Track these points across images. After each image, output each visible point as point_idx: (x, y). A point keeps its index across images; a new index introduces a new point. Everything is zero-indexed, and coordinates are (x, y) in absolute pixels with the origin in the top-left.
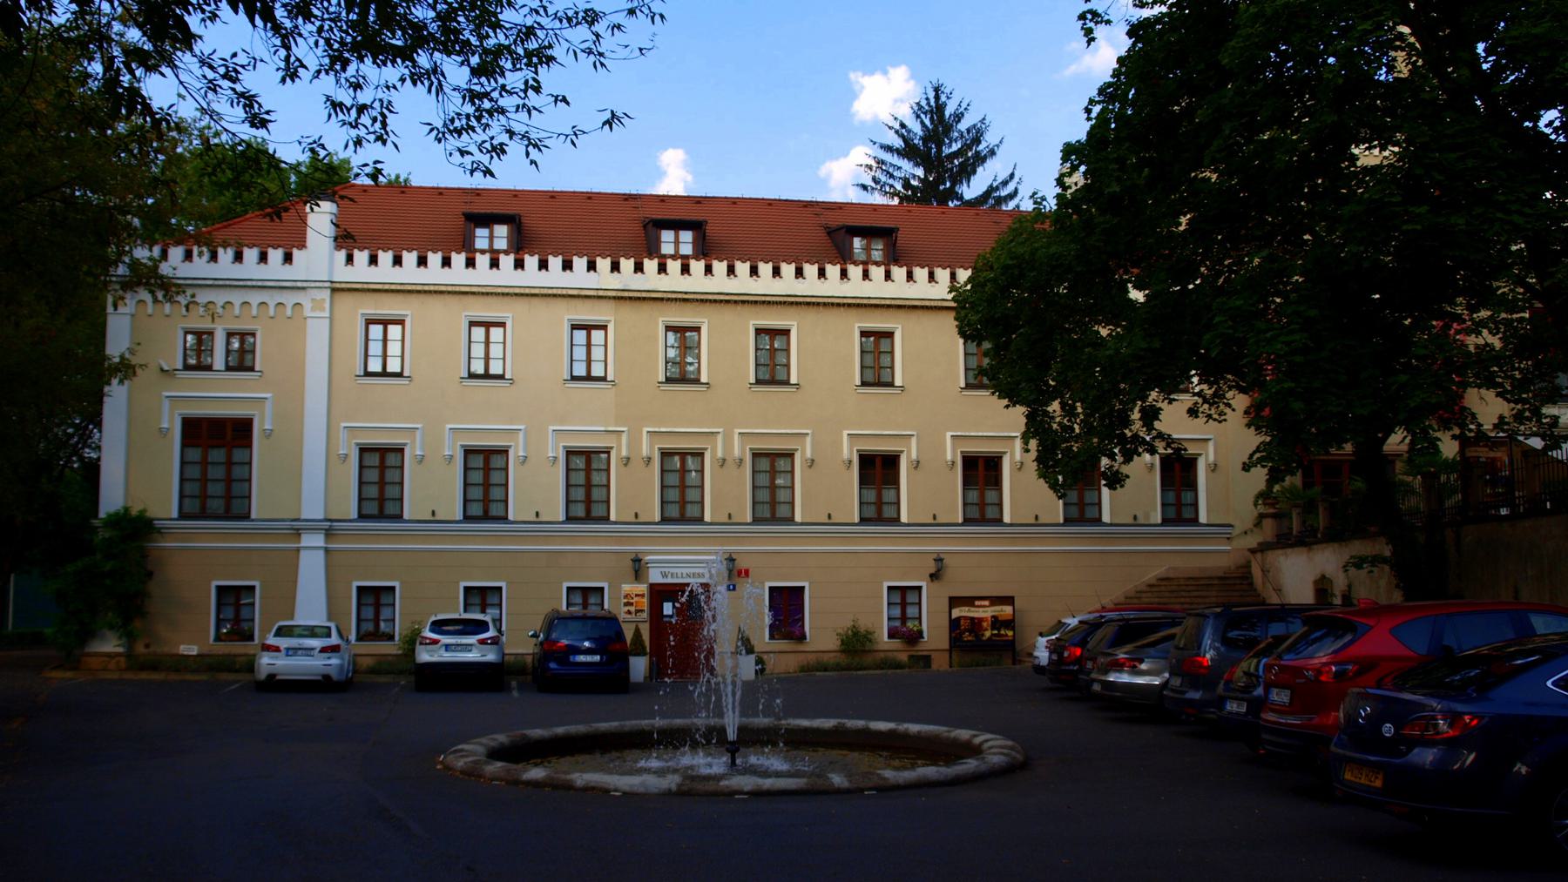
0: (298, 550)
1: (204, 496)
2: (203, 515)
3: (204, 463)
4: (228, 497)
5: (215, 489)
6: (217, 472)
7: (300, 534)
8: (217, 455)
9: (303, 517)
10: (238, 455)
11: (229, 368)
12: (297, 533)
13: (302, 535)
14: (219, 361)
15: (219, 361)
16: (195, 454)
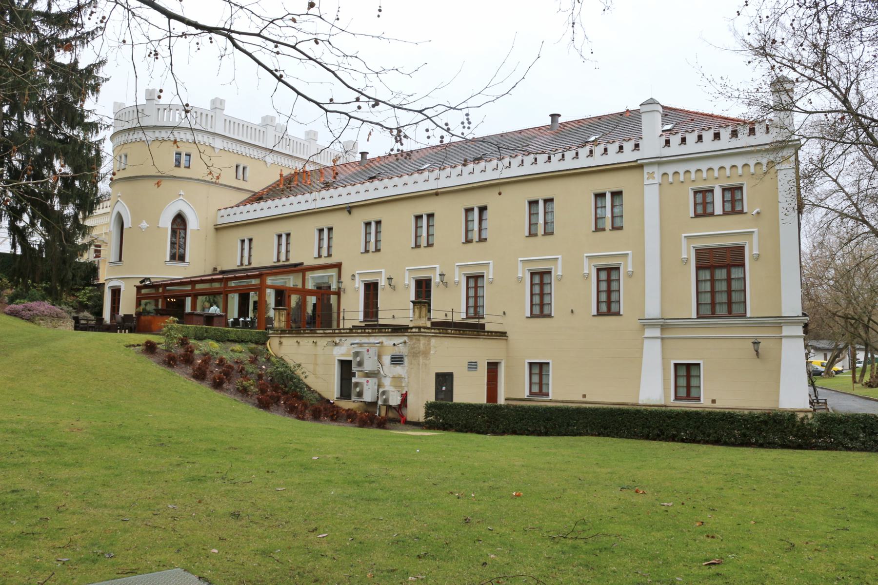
0: (781, 338)
1: (713, 304)
2: (713, 315)
3: (713, 281)
4: (730, 303)
5: (722, 298)
6: (722, 286)
8: (721, 274)
9: (783, 315)
10: (736, 273)
11: (725, 213)
12: (779, 326)
13: (783, 327)
14: (718, 210)
15: (718, 210)
16: (706, 275)
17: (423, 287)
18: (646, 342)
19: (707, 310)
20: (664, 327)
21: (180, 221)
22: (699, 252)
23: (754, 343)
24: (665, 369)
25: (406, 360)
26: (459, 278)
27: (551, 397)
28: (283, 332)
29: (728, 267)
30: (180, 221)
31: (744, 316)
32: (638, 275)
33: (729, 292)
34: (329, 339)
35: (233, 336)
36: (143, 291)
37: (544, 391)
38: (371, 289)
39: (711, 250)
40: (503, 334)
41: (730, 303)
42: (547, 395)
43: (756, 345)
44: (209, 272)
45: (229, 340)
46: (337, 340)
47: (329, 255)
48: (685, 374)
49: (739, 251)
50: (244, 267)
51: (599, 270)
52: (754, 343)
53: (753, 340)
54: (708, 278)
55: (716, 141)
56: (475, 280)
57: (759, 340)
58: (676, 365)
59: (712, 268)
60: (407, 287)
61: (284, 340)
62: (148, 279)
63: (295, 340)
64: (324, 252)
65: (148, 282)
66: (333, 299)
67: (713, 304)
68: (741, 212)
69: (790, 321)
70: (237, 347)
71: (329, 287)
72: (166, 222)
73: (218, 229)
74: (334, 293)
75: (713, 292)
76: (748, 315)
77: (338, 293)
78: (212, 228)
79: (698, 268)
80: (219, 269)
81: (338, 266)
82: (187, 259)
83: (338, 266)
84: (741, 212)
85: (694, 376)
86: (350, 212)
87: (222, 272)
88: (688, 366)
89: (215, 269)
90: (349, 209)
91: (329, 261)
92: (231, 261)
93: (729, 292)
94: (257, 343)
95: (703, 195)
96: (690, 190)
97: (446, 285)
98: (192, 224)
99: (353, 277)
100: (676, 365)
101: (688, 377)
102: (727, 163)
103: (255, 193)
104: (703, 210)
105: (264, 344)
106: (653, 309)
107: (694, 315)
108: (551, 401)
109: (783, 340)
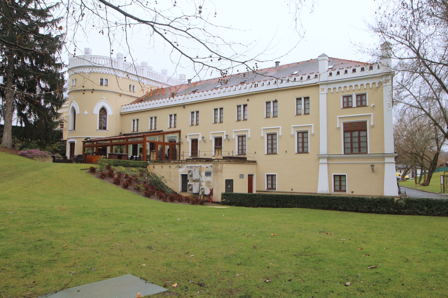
0: (384, 163)
1: (352, 148)
2: (352, 153)
3: (351, 137)
4: (360, 148)
5: (356, 145)
6: (356, 140)
7: (385, 158)
8: (356, 134)
9: (385, 153)
10: (362, 134)
11: (358, 106)
12: (383, 158)
14: (354, 105)
16: (348, 135)
17: (218, 141)
18: (320, 166)
19: (349, 150)
20: (328, 159)
21: (103, 111)
22: (345, 124)
23: (371, 166)
24: (329, 177)
25: (212, 174)
26: (234, 137)
27: (277, 190)
28: (155, 162)
29: (359, 131)
30: (103, 111)
31: (366, 153)
32: (317, 135)
33: (359, 142)
34: (177, 165)
35: (132, 164)
36: (86, 144)
37: (274, 187)
38: (195, 142)
39: (351, 123)
40: (255, 162)
41: (360, 148)
42: (275, 189)
43: (372, 166)
44: (118, 135)
45: (130, 166)
46: (180, 165)
47: (175, 127)
48: (339, 180)
49: (365, 123)
50: (135, 132)
51: (298, 133)
52: (371, 166)
53: (371, 164)
54: (349, 136)
55: (354, 73)
56: (242, 138)
57: (374, 164)
58: (334, 176)
59: (351, 131)
60: (211, 141)
61: (156, 166)
62: (89, 138)
63: (160, 165)
64: (173, 126)
65: (89, 140)
66: (177, 147)
67: (352, 148)
68: (365, 106)
69: (389, 155)
70: (134, 169)
71: (175, 141)
72: (97, 111)
73: (122, 115)
74: (178, 144)
75: (352, 142)
76: (368, 153)
77: (179, 144)
78: (119, 114)
79: (345, 132)
80: (123, 133)
81: (179, 132)
82: (107, 128)
83: (179, 132)
84: (365, 106)
85: (343, 181)
86: (184, 107)
87: (124, 135)
88: (340, 176)
89: (121, 133)
90: (184, 106)
91: (175, 130)
92: (129, 130)
93: (359, 142)
94: (143, 167)
95: (348, 97)
96: (341, 96)
97: (229, 140)
98: (110, 112)
99: (186, 137)
100: (334, 176)
101: (340, 181)
102: (359, 83)
103: (139, 98)
104: (347, 105)
105: (146, 167)
106: (323, 150)
107: (343, 153)
108: (277, 192)
109: (385, 164)
